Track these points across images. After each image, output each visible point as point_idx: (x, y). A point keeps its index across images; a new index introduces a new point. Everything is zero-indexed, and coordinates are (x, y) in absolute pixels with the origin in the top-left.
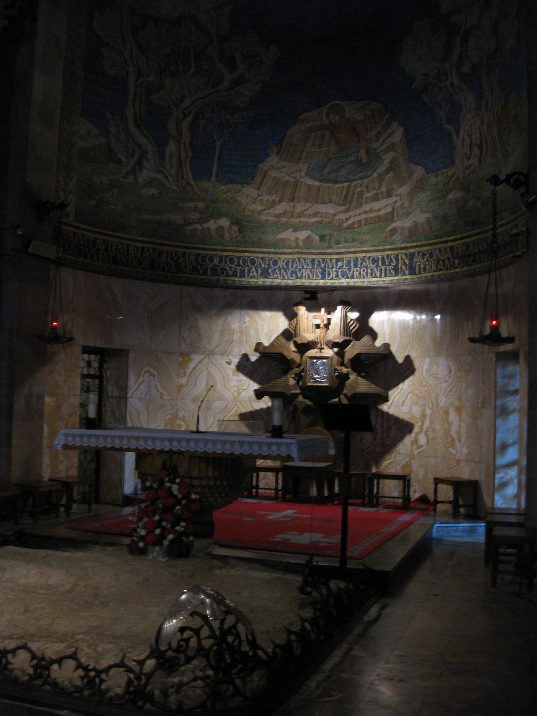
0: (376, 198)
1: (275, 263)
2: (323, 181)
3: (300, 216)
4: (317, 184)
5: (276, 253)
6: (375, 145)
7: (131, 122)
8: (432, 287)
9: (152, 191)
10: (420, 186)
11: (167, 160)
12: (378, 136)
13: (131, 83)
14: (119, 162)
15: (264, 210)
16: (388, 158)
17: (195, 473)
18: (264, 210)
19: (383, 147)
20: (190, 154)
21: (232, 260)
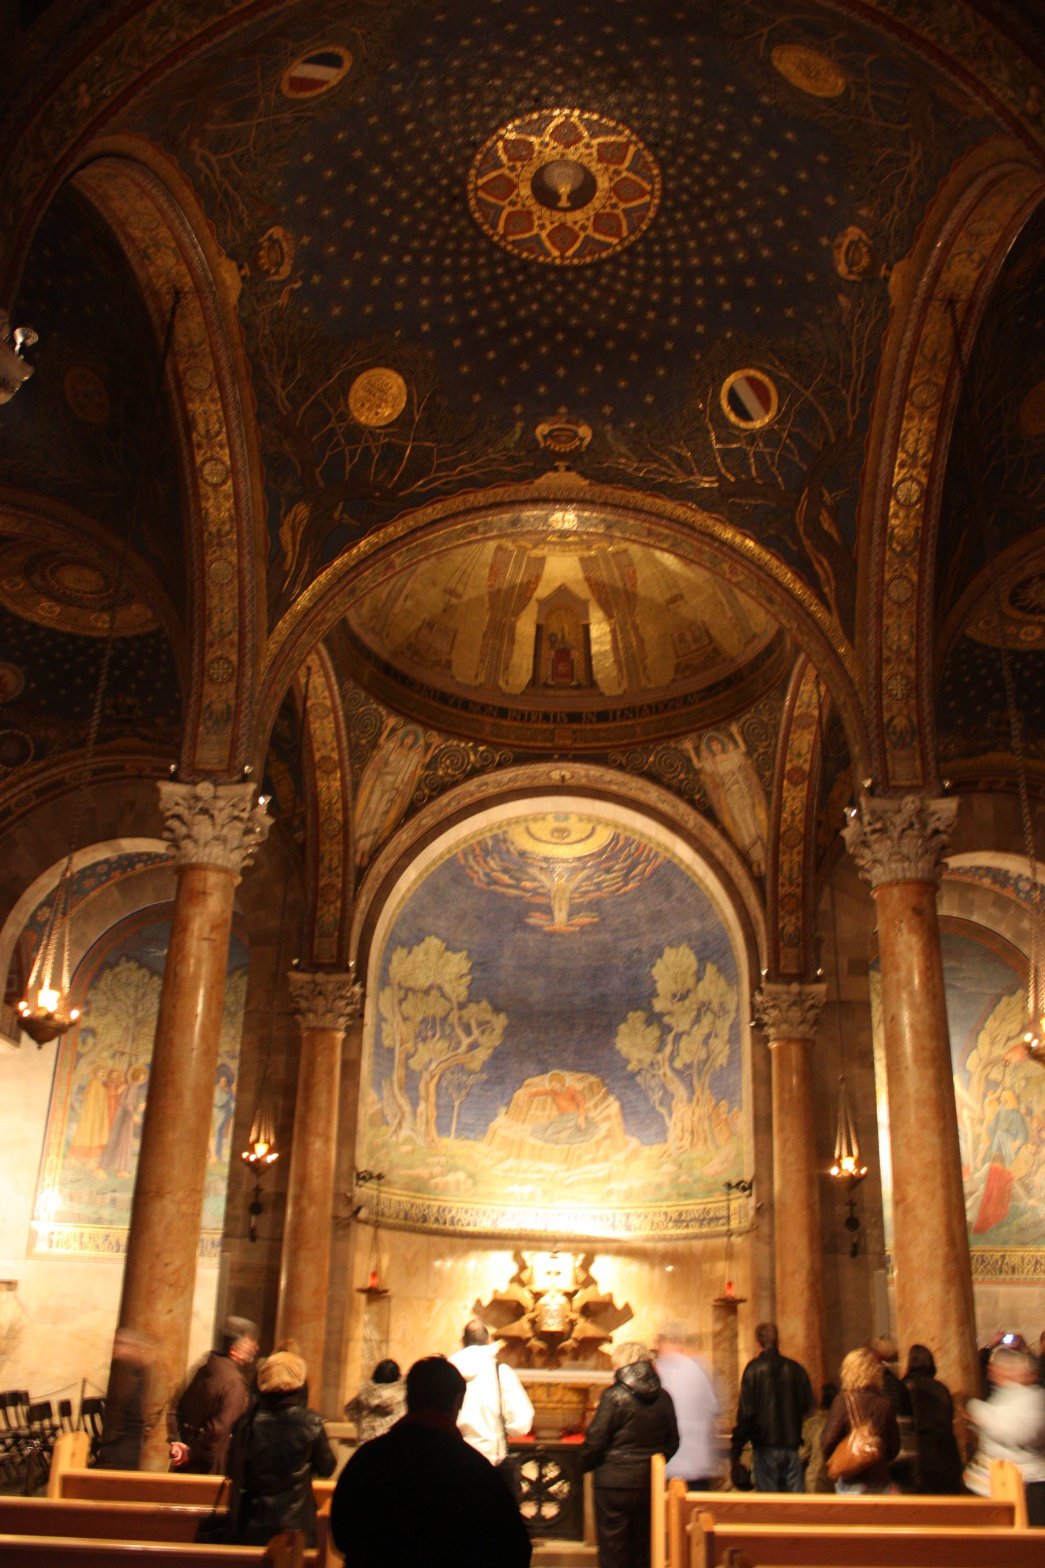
0: (594, 1161)
1: (503, 1214)
2: (546, 1141)
3: (525, 1171)
4: (540, 1144)
5: (504, 1205)
6: (592, 1114)
7: (396, 1086)
8: (649, 1245)
9: (406, 1148)
10: (635, 1154)
11: (418, 1119)
12: (596, 1106)
13: (397, 1052)
14: (387, 1124)
15: (493, 1166)
16: (605, 1127)
17: (566, 1398)
18: (493, 1166)
19: (601, 1116)
20: (435, 1113)
21: (466, 1212)
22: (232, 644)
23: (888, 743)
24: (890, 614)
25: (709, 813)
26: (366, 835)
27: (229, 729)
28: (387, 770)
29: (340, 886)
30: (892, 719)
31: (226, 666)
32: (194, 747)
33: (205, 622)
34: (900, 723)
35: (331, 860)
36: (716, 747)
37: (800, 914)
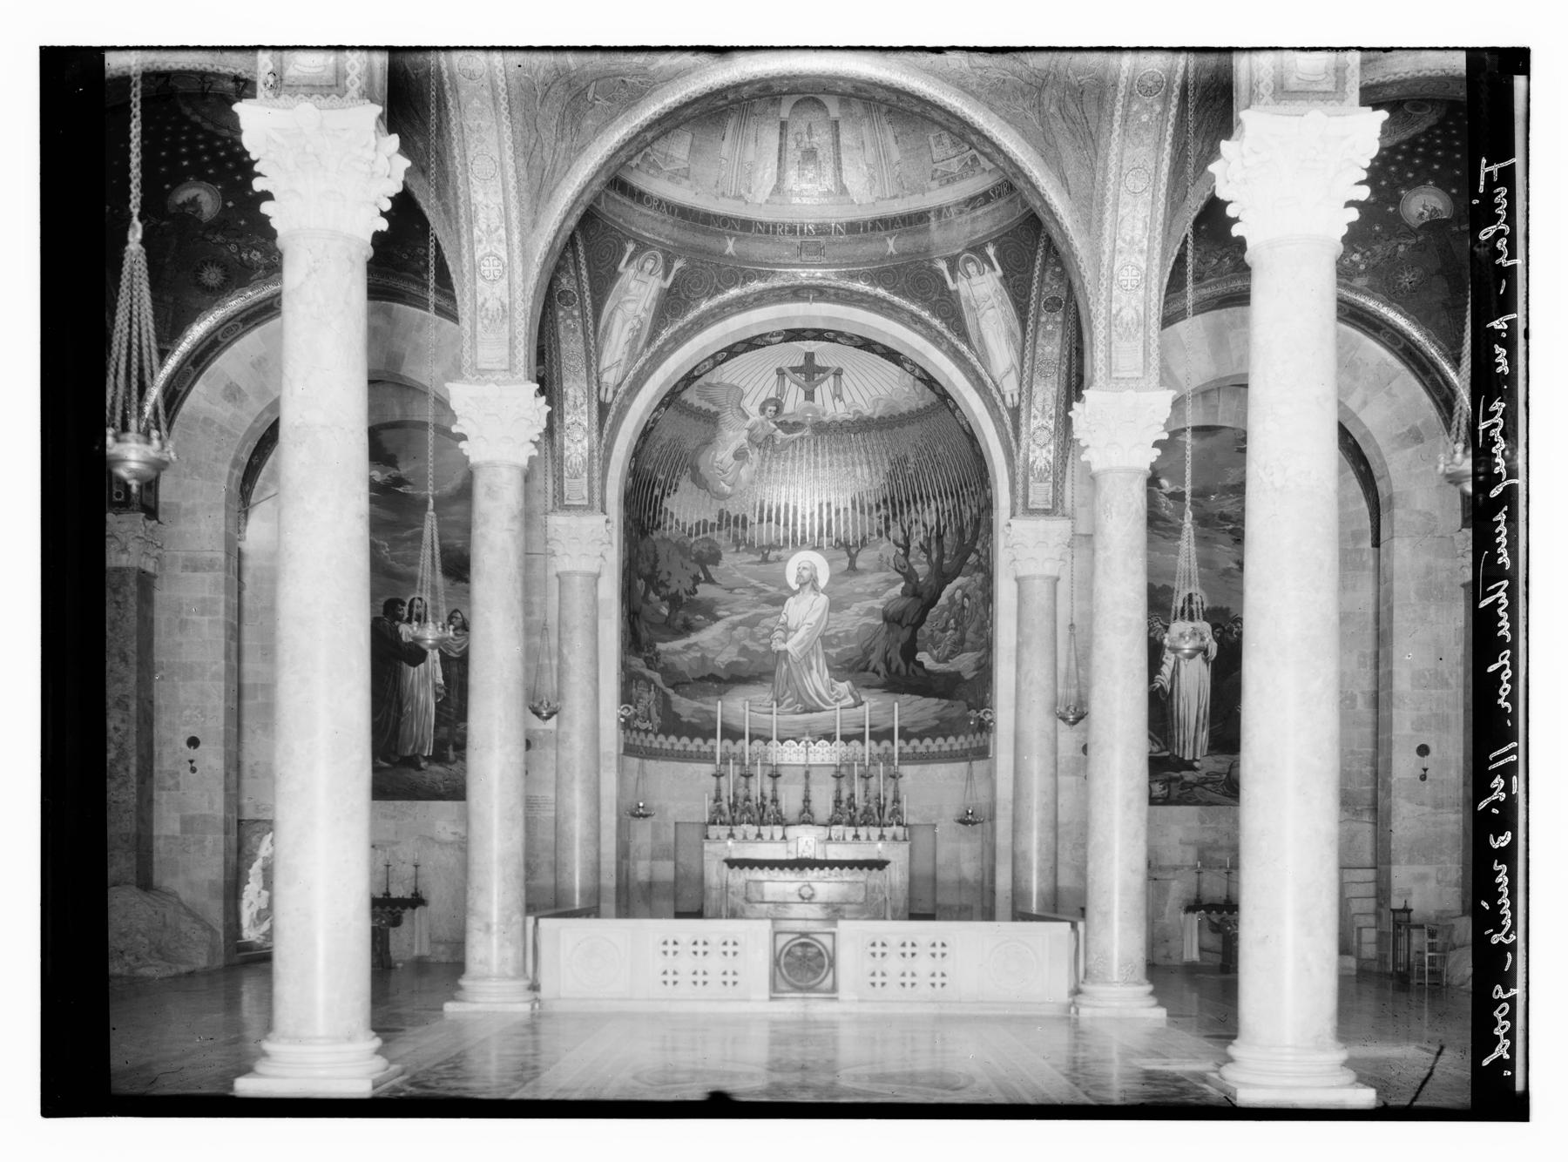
22: (500, 241)
23: (1114, 333)
24: (1126, 204)
25: (964, 335)
26: (610, 368)
27: (506, 327)
28: (627, 298)
29: (586, 424)
30: (1120, 310)
31: (496, 263)
32: (474, 346)
33: (471, 222)
34: (1128, 315)
35: (575, 397)
36: (971, 268)
37: (1052, 447)
